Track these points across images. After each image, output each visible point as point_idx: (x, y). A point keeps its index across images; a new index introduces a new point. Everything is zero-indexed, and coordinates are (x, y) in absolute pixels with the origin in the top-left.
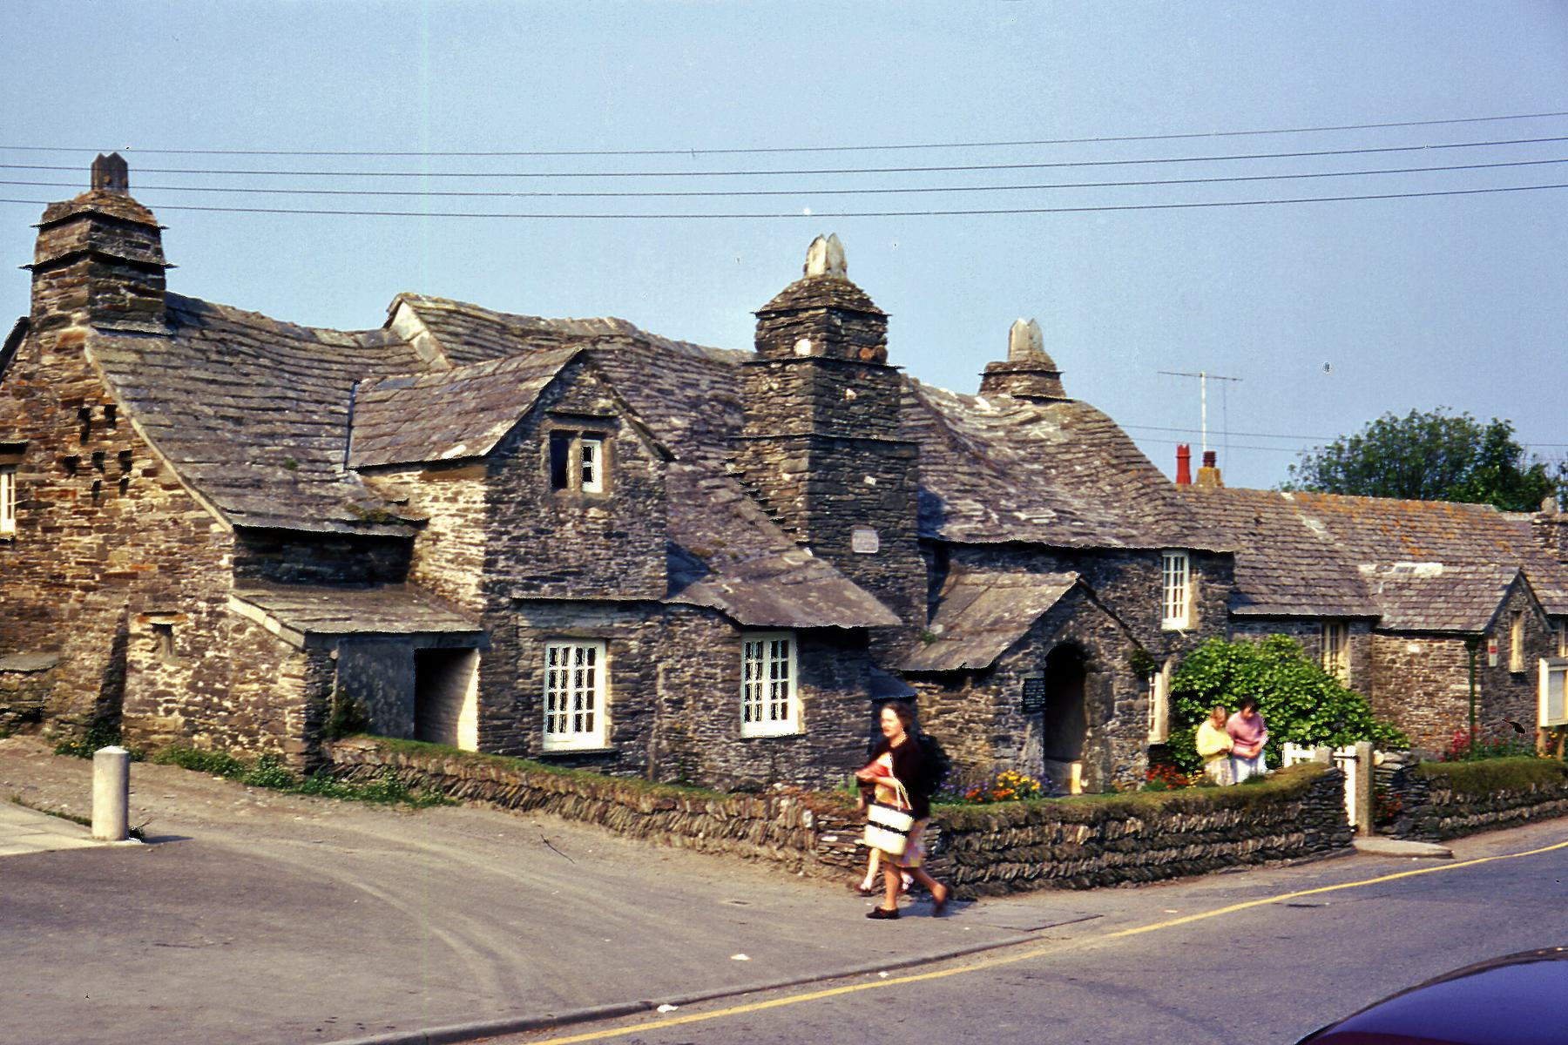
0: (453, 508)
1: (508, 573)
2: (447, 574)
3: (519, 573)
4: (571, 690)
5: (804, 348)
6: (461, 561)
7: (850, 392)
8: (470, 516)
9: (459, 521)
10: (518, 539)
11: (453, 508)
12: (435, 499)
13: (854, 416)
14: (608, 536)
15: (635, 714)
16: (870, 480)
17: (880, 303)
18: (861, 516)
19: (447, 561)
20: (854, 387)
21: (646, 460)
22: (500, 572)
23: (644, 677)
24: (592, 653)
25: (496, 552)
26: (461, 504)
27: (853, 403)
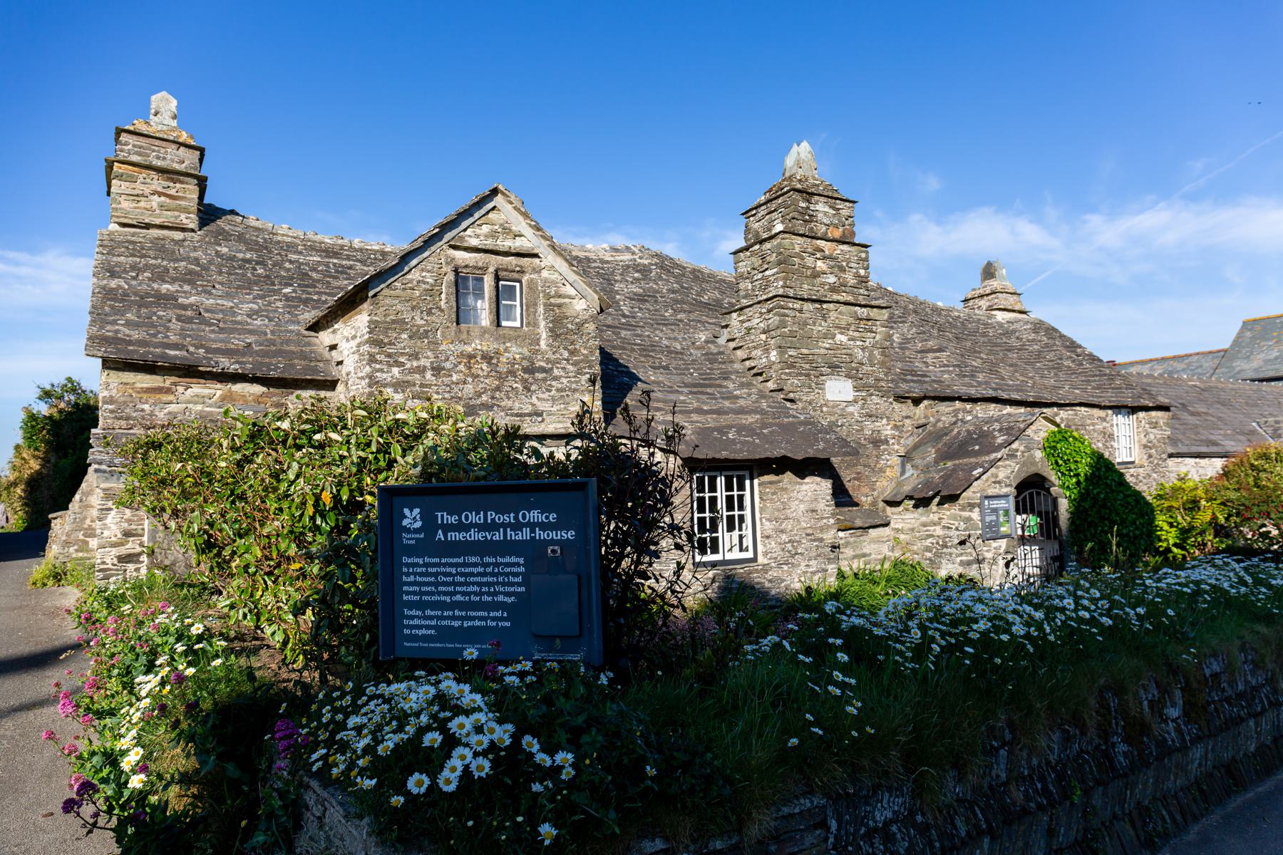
10: (413, 371)
13: (823, 284)
16: (841, 338)
18: (834, 368)
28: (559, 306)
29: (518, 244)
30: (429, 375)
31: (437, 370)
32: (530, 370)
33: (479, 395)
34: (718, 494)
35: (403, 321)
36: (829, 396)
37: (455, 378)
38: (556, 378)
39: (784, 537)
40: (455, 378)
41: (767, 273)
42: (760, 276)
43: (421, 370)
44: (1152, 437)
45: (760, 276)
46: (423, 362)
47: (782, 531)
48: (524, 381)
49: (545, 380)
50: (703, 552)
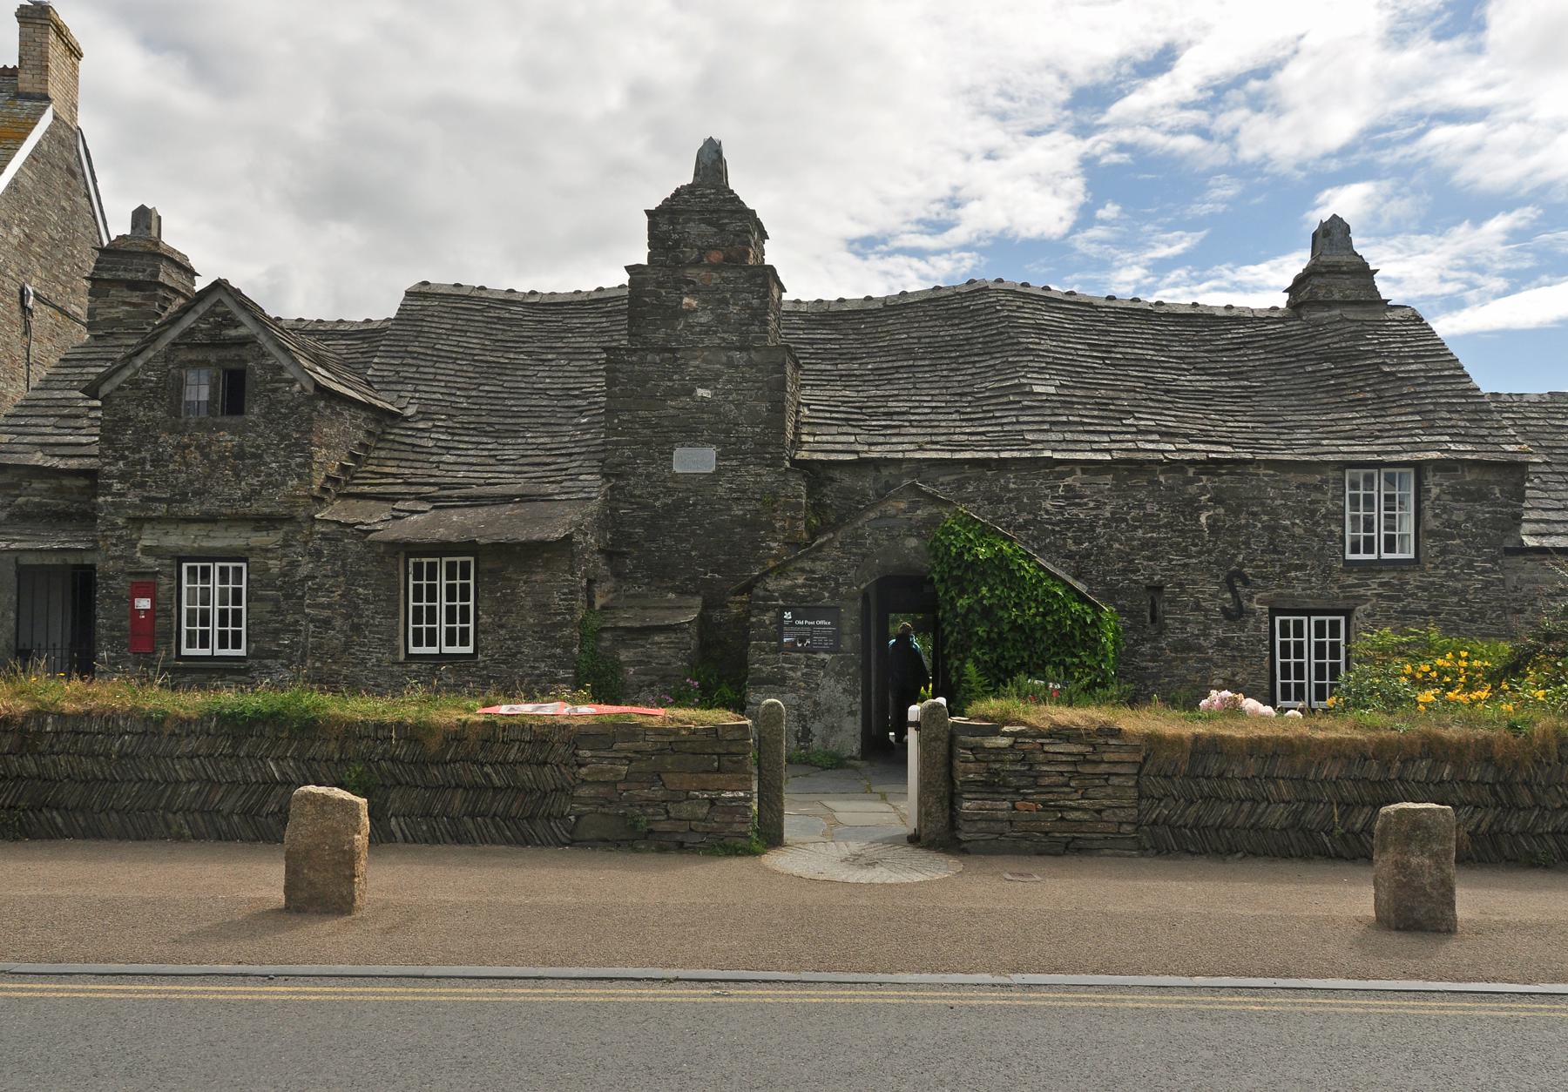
1: (124, 495)
3: (132, 498)
7: (686, 300)
10: (134, 463)
13: (689, 326)
15: (276, 632)
16: (701, 392)
18: (691, 434)
21: (292, 382)
28: (275, 390)
29: (242, 331)
30: (148, 467)
31: (156, 462)
32: (240, 455)
33: (191, 482)
34: (444, 582)
35: (129, 419)
36: (677, 469)
37: (171, 467)
38: (265, 464)
39: (502, 632)
40: (171, 467)
43: (143, 462)
44: (1458, 516)
47: (502, 626)
48: (234, 469)
49: (254, 466)
50: (418, 643)
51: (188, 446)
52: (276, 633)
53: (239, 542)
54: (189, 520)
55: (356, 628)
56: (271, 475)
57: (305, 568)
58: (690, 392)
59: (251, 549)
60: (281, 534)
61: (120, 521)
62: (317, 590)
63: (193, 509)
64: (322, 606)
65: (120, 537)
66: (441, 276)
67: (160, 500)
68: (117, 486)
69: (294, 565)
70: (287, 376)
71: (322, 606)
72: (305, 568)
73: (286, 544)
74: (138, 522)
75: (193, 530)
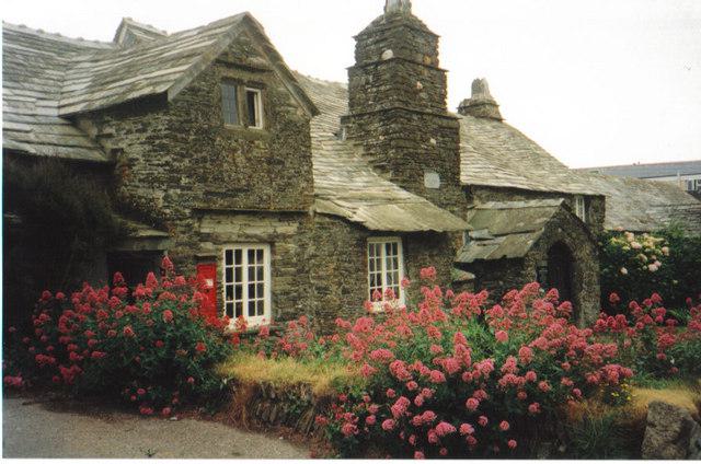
0: (143, 137)
1: (190, 189)
2: (141, 192)
4: (245, 283)
5: (388, 54)
6: (152, 181)
7: (419, 84)
8: (157, 142)
9: (147, 147)
10: (197, 161)
11: (143, 137)
12: (129, 132)
14: (269, 163)
16: (433, 141)
17: (432, 28)
19: (140, 181)
20: (422, 80)
22: (183, 189)
23: (299, 272)
24: (260, 253)
25: (178, 171)
26: (149, 133)
27: (421, 91)
41: (383, 88)
42: (375, 89)
43: (204, 160)
45: (375, 89)
46: (204, 154)
48: (269, 172)
51: (235, 150)
52: (294, 301)
53: (271, 231)
54: (235, 213)
55: (345, 291)
56: (289, 178)
57: (311, 249)
58: (428, 140)
59: (277, 236)
60: (296, 225)
61: (187, 211)
62: (318, 266)
63: (241, 202)
64: (320, 278)
65: (188, 225)
66: (142, 18)
67: (217, 194)
68: (184, 181)
69: (303, 246)
70: (293, 102)
71: (320, 278)
72: (311, 249)
73: (300, 232)
74: (199, 214)
75: (240, 220)
